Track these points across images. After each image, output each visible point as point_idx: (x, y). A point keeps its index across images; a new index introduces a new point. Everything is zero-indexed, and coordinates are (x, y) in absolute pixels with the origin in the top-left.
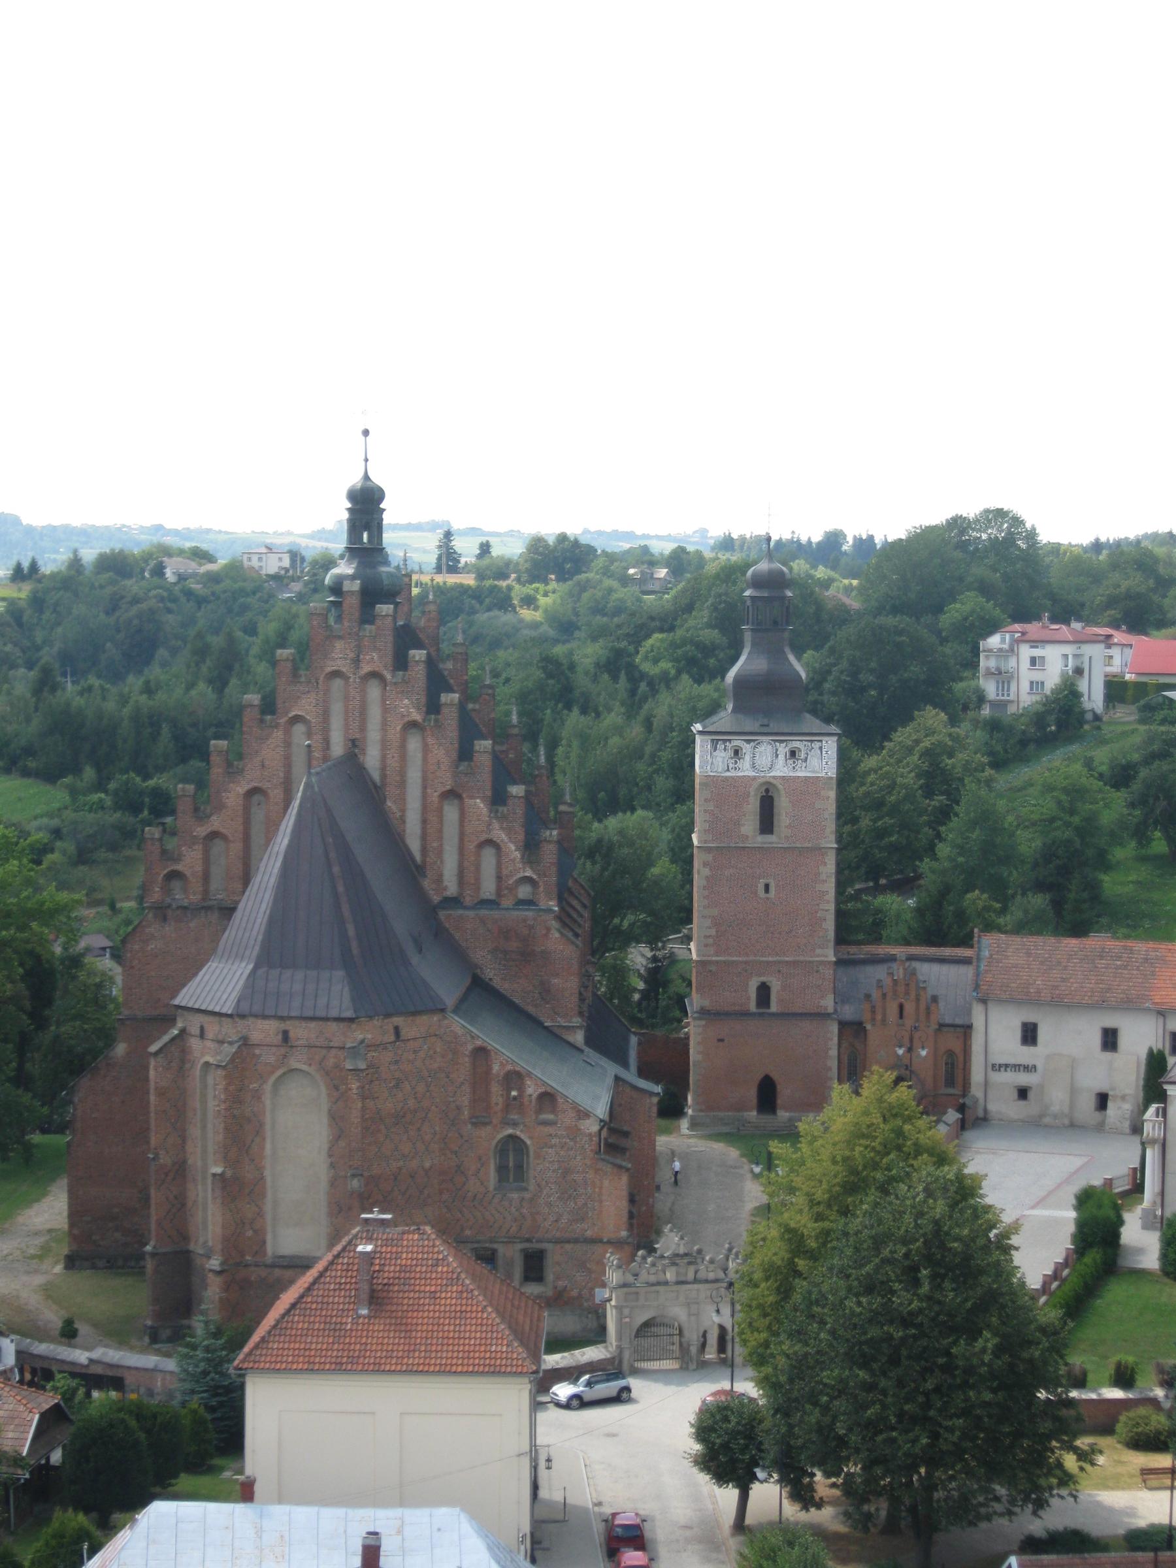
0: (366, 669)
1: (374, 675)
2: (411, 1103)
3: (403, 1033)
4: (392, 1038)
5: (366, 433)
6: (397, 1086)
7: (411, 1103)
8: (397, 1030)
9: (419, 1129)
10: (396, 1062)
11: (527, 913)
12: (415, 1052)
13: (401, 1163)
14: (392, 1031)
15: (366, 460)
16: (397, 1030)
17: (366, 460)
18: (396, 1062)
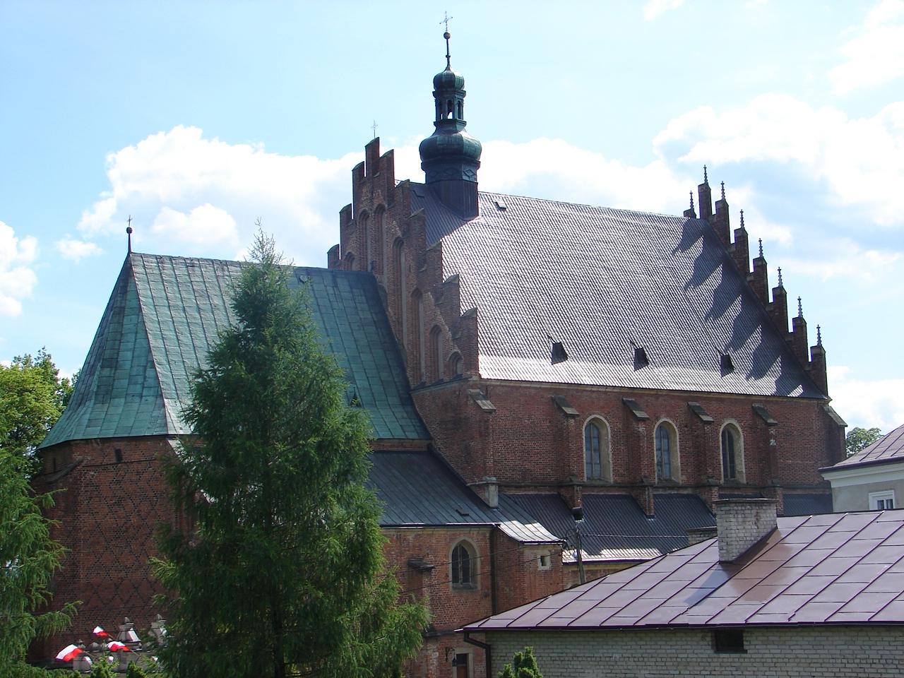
0: (376, 202)
1: (381, 209)
2: (134, 520)
3: (126, 456)
4: (114, 460)
5: (447, 36)
6: (118, 503)
7: (134, 520)
8: (119, 454)
9: (143, 544)
10: (118, 482)
11: (454, 385)
12: (138, 473)
13: (122, 574)
14: (113, 454)
15: (448, 57)
16: (119, 454)
17: (448, 57)
18: (118, 482)
